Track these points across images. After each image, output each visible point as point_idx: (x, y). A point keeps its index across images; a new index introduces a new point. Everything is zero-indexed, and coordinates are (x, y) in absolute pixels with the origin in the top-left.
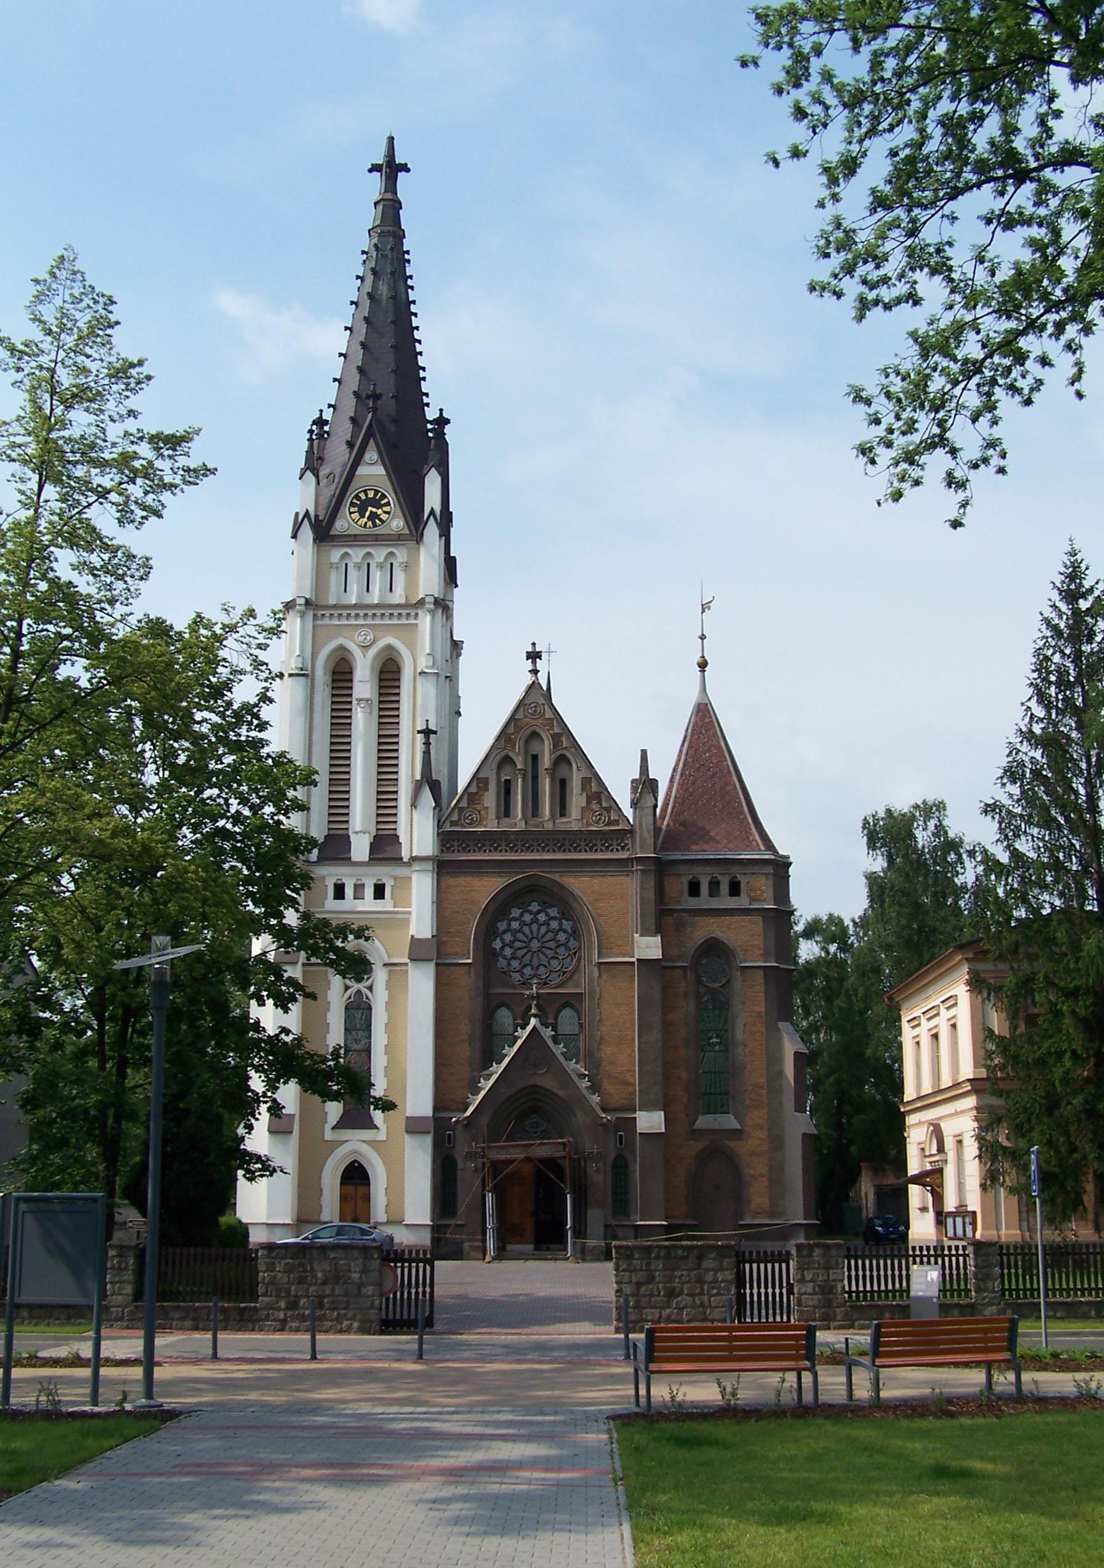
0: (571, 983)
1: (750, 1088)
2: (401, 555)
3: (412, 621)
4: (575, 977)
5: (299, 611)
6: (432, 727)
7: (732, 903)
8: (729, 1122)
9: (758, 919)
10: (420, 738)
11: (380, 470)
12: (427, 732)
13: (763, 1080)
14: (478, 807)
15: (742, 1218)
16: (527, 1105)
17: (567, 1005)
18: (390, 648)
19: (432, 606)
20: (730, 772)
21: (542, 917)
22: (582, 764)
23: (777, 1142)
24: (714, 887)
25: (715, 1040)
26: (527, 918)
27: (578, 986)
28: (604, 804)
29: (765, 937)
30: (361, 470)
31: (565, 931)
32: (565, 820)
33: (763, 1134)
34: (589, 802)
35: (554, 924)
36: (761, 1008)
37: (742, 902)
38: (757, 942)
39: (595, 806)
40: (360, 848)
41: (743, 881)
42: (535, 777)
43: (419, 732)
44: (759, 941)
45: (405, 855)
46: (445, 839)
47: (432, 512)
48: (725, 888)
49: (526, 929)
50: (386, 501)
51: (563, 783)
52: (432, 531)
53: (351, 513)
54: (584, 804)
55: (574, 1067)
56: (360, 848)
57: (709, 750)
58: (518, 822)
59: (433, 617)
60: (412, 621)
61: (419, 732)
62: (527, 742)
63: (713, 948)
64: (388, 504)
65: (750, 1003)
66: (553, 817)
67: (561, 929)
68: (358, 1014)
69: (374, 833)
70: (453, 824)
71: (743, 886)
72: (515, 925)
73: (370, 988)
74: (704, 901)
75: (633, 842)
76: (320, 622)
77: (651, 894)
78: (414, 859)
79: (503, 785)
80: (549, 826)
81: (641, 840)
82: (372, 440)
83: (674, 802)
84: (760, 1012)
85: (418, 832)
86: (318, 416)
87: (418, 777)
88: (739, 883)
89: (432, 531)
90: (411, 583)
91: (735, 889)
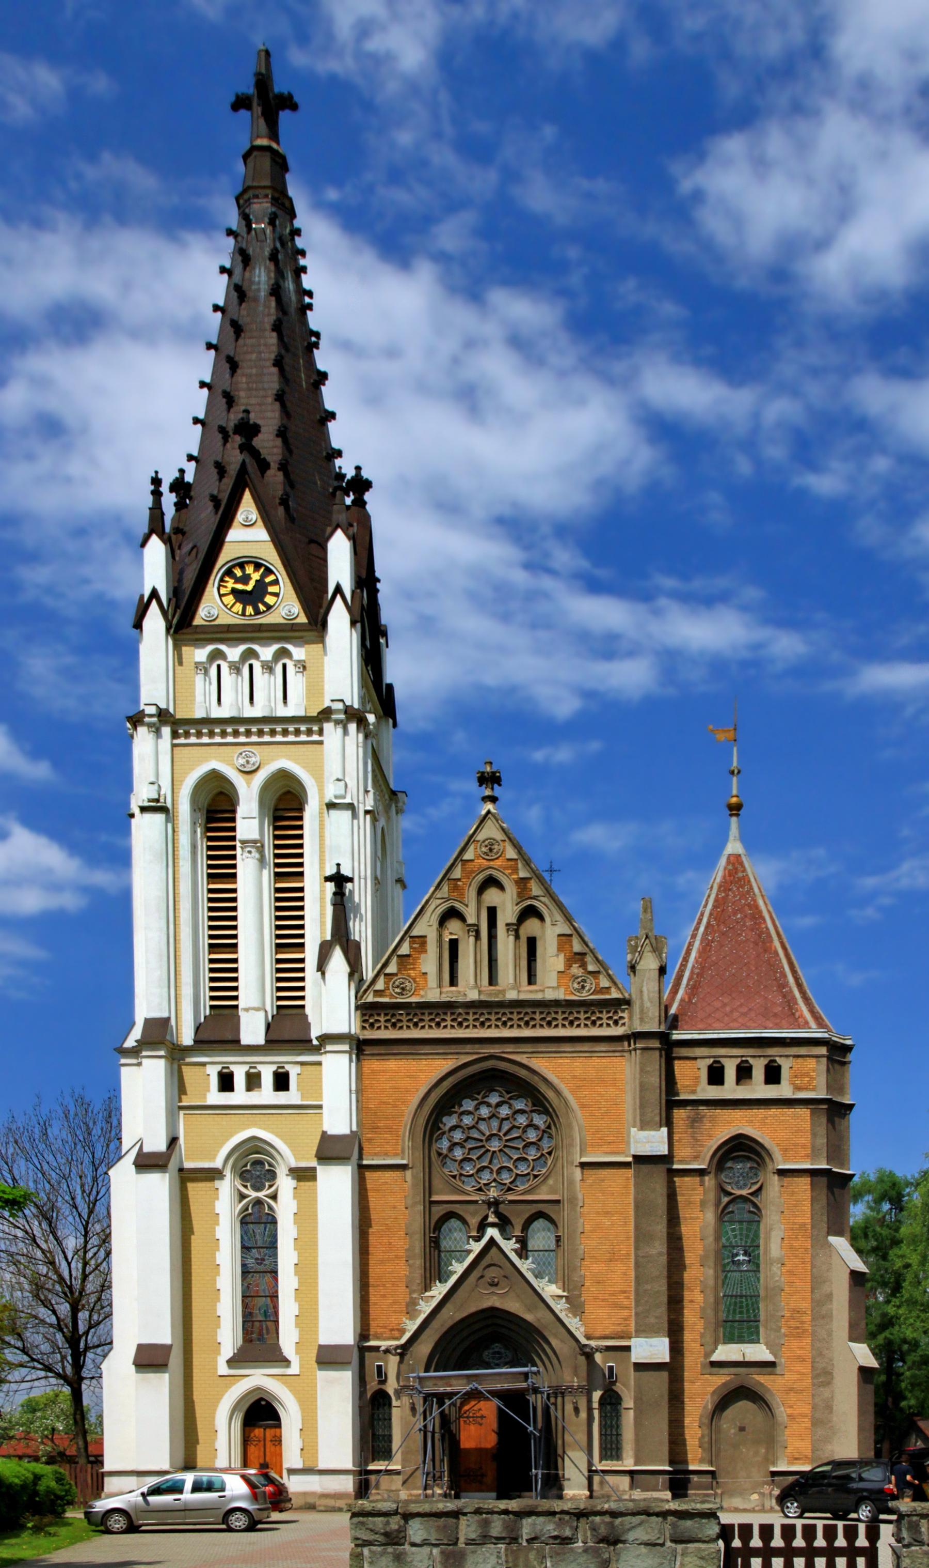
0: (544, 1188)
1: (787, 1314)
2: (298, 653)
3: (315, 737)
4: (551, 1182)
5: (150, 725)
6: (346, 871)
7: (771, 1092)
8: (758, 1352)
9: (804, 1113)
10: (330, 887)
11: (261, 534)
12: (339, 879)
13: (806, 1305)
14: (412, 973)
15: (774, 1464)
16: (486, 1336)
17: (540, 1215)
18: (283, 776)
19: (342, 716)
20: (769, 936)
21: (504, 1111)
22: (558, 917)
23: (823, 1376)
24: (744, 1073)
25: (741, 1258)
26: (484, 1112)
27: (553, 1191)
28: (591, 968)
29: (814, 1135)
30: (234, 534)
31: (536, 1128)
32: (532, 988)
33: (806, 1368)
34: (568, 966)
35: (522, 1120)
36: (805, 1217)
37: (784, 1090)
38: (803, 1141)
39: (576, 970)
40: (252, 1030)
41: (786, 1065)
42: (492, 937)
43: (328, 879)
44: (805, 1139)
45: (314, 1033)
46: (367, 1011)
47: (338, 590)
48: (758, 1073)
49: (483, 1126)
50: (271, 578)
51: (532, 943)
52: (339, 618)
53: (221, 596)
54: (562, 968)
55: (550, 1290)
56: (252, 1030)
57: (740, 910)
58: (470, 987)
59: (346, 732)
60: (315, 737)
61: (328, 879)
62: (481, 890)
63: (742, 1150)
64: (276, 582)
65: (787, 1211)
66: (516, 986)
67: (531, 1125)
68: (259, 1229)
69: (270, 1009)
70: (378, 993)
71: (785, 1074)
72: (467, 1120)
73: (274, 1197)
74: (730, 1089)
75: (630, 1018)
76: (182, 741)
77: (655, 1079)
78: (326, 1038)
79: (446, 947)
80: (512, 995)
81: (642, 1011)
82: (247, 496)
83: (692, 972)
84: (804, 1224)
85: (331, 1004)
86: (177, 475)
87: (329, 938)
88: (779, 1067)
89: (339, 618)
90: (314, 689)
91: (773, 1075)
